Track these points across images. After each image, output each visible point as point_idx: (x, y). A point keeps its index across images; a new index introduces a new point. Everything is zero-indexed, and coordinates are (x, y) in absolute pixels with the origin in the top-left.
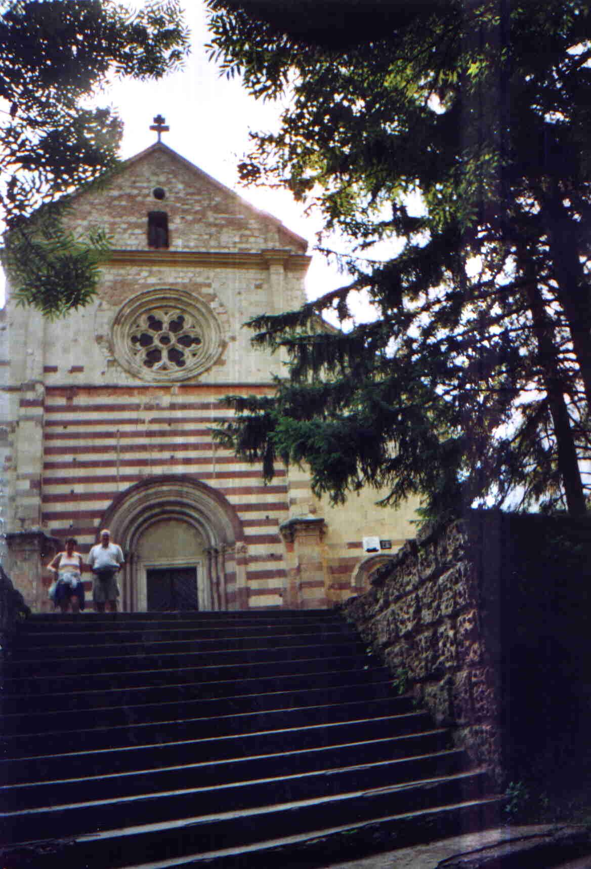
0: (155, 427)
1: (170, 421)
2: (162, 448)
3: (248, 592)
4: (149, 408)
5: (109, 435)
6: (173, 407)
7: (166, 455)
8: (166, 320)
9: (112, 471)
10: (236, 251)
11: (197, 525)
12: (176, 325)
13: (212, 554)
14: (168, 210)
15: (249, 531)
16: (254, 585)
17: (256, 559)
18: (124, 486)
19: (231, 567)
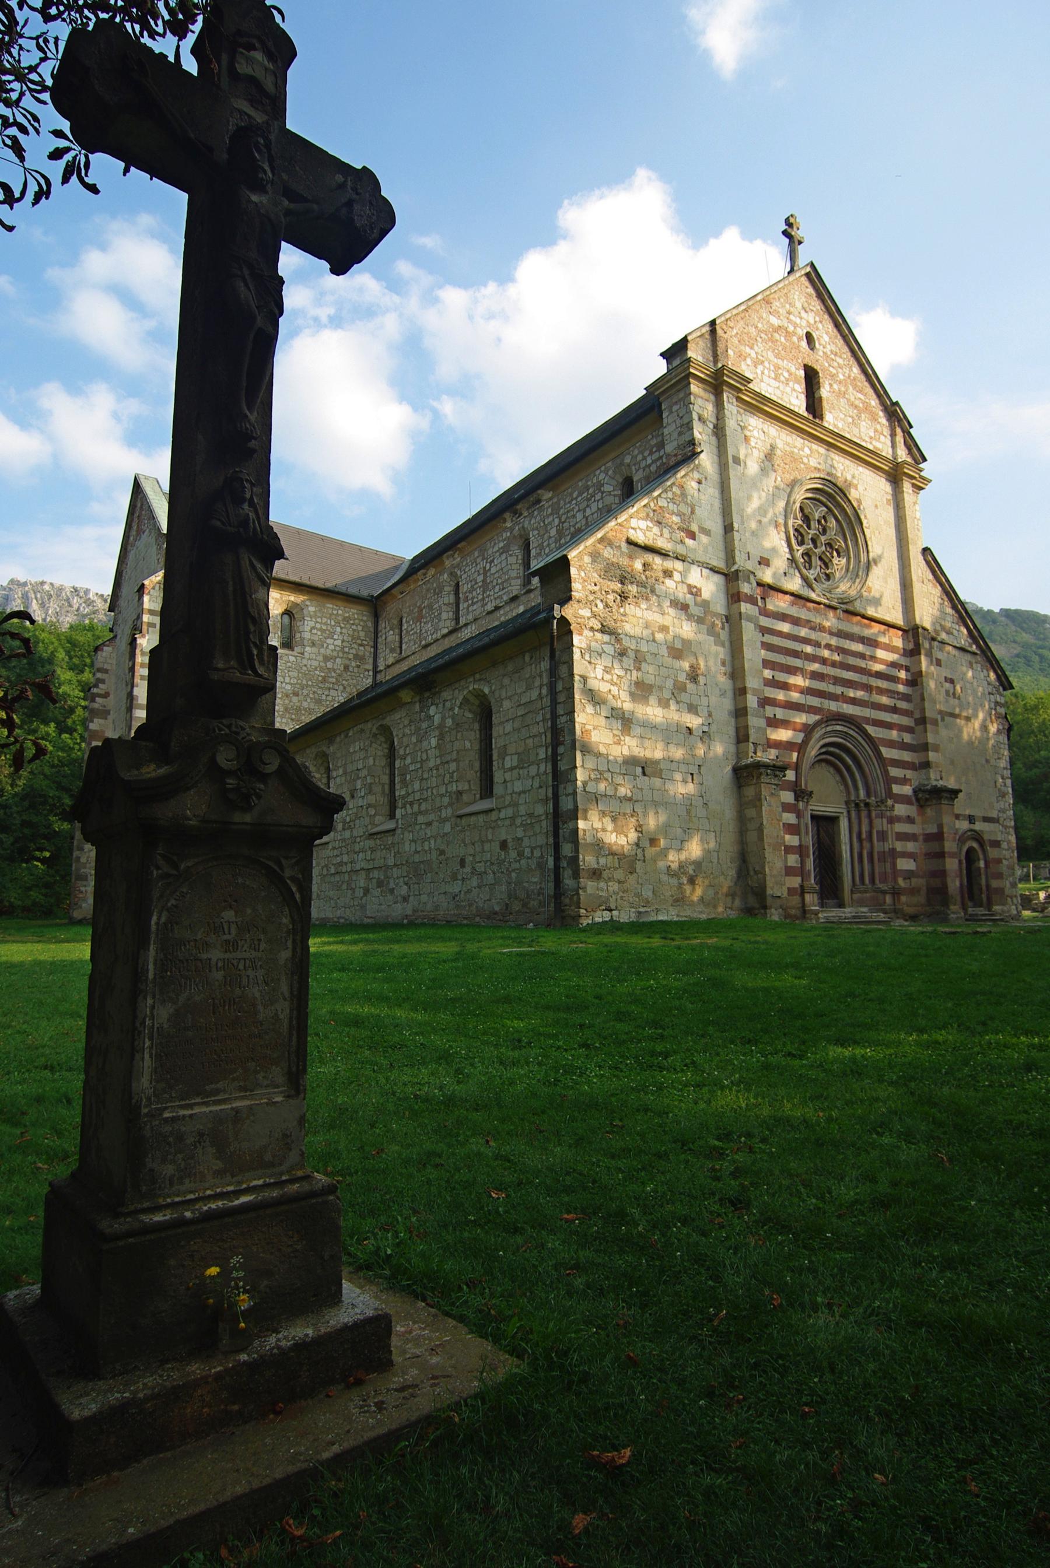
3: (893, 854)
13: (856, 806)
14: (817, 367)
15: (896, 789)
16: (899, 846)
17: (899, 819)
18: (813, 719)
19: (880, 824)
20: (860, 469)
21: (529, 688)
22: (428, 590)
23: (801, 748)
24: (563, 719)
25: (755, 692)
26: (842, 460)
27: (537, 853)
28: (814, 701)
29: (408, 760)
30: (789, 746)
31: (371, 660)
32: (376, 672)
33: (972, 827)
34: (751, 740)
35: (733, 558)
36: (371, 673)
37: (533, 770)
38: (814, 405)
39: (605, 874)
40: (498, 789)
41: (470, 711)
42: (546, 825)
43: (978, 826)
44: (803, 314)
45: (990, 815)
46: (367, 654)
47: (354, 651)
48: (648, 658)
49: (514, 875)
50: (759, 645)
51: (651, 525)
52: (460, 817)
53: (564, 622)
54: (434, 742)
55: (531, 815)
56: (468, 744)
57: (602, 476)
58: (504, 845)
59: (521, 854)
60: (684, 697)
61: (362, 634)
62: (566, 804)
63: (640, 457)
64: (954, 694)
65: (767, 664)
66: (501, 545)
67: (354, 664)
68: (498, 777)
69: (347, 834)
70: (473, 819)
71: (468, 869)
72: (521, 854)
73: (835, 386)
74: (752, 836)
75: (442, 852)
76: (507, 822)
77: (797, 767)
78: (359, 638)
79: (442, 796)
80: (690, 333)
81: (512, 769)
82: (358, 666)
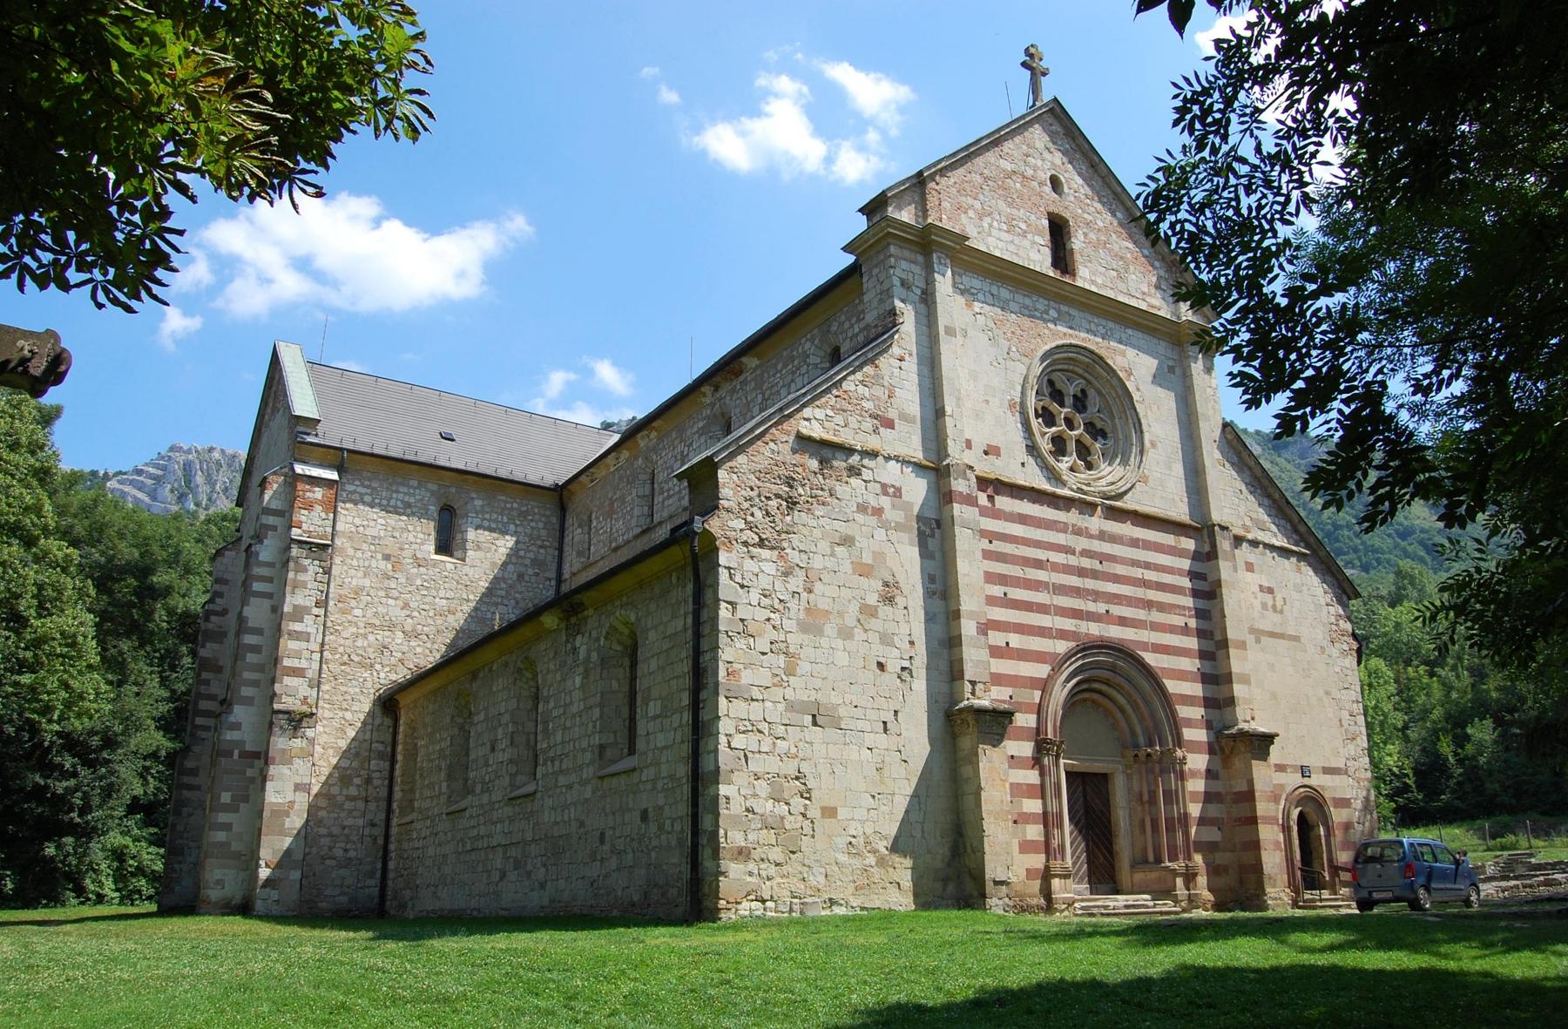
0: (1086, 563)
1: (1103, 558)
2: (1097, 596)
4: (1078, 532)
5: (1038, 564)
6: (1103, 536)
7: (1101, 608)
8: (1071, 390)
9: (1045, 621)
10: (1143, 306)
11: (1119, 715)
12: (1080, 403)
14: (1067, 215)
18: (1062, 647)
20: (1130, 331)
21: (674, 616)
22: (621, 478)
23: (1045, 685)
24: (707, 656)
25: (972, 615)
26: (1103, 322)
27: (677, 827)
28: (1068, 624)
29: (552, 704)
30: (1033, 683)
31: (554, 567)
32: (559, 581)
33: (1306, 781)
34: (967, 677)
35: (946, 448)
36: (553, 583)
37: (676, 719)
38: (1062, 257)
39: (756, 855)
40: (640, 745)
41: (619, 643)
42: (686, 789)
43: (1315, 781)
44: (1046, 155)
45: (1333, 765)
46: (550, 558)
47: (531, 555)
48: (826, 577)
49: (653, 854)
50: (979, 555)
51: (831, 413)
52: (602, 778)
53: (709, 538)
54: (578, 680)
55: (672, 777)
56: (615, 685)
57: (807, 346)
58: (644, 816)
59: (661, 828)
60: (874, 624)
61: (543, 533)
62: (706, 764)
63: (847, 325)
64: (1274, 607)
65: (991, 578)
66: (701, 424)
67: (530, 571)
68: (642, 727)
69: (485, 799)
70: (615, 780)
71: (606, 847)
72: (661, 828)
73: (1092, 236)
74: (969, 801)
75: (582, 824)
76: (649, 786)
77: (1040, 710)
78: (539, 537)
79: (584, 750)
80: (890, 189)
81: (656, 717)
82: (537, 575)
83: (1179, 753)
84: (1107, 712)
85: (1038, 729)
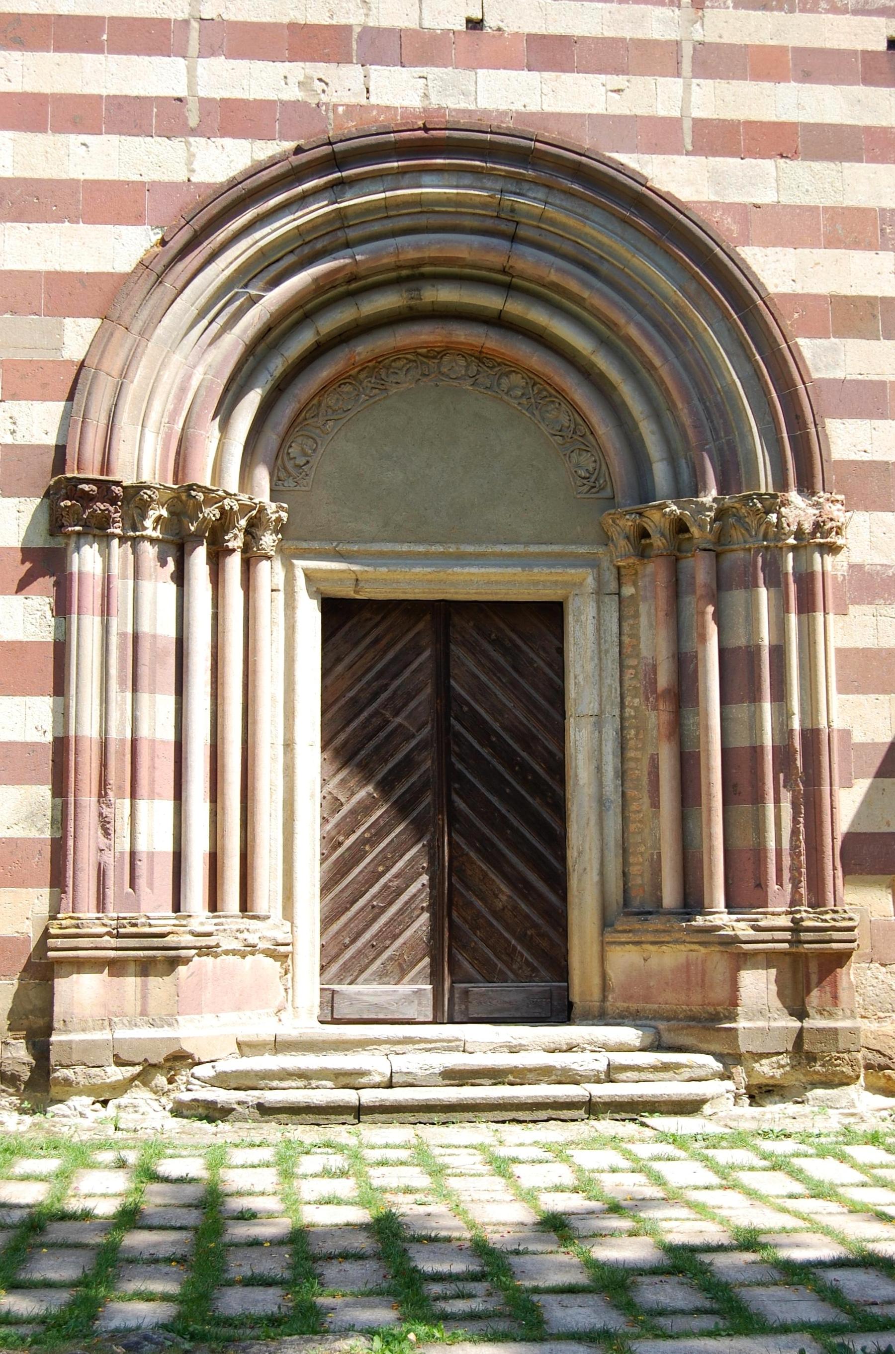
11: (580, 394)
18: (224, 160)
23: (111, 300)
30: (63, 293)
83: (798, 510)
84: (544, 393)
85: (60, 450)
